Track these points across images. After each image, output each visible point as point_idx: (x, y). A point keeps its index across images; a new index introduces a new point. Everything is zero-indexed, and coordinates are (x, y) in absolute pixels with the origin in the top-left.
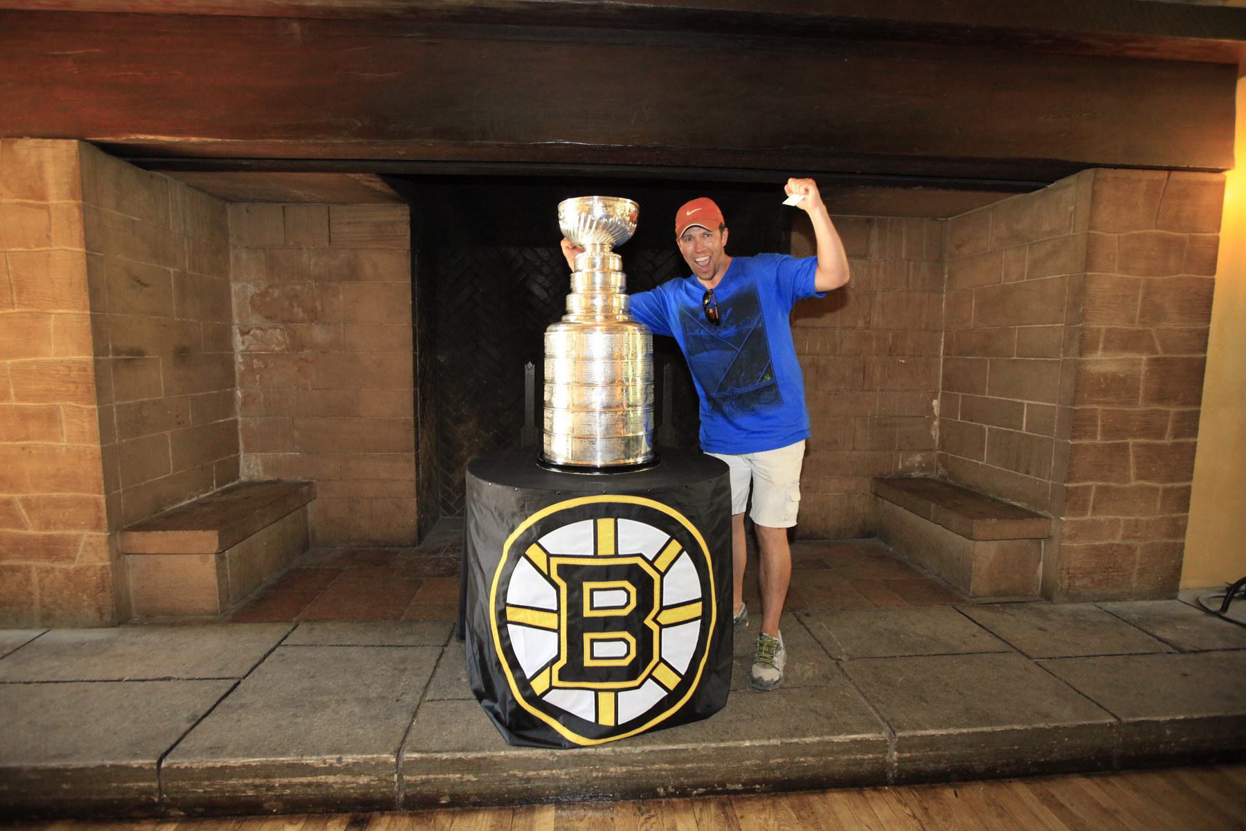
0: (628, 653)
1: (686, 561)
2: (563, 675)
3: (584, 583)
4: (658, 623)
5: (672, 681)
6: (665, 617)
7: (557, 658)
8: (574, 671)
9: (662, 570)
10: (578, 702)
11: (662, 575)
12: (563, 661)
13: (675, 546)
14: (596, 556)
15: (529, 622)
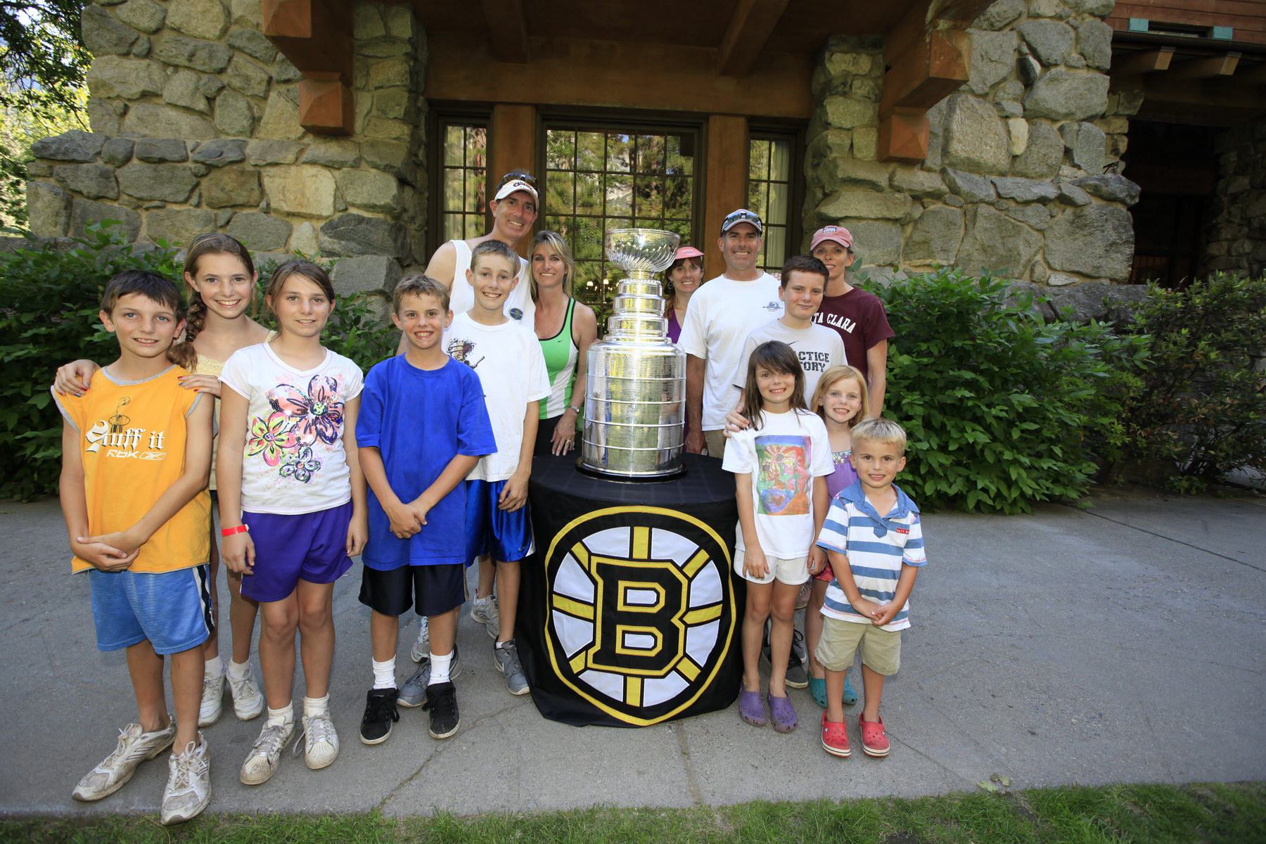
0: (655, 646)
1: (712, 569)
2: (598, 658)
3: (620, 582)
4: (684, 623)
5: (693, 673)
6: (690, 618)
7: (592, 644)
8: (607, 656)
9: (690, 575)
10: (608, 682)
11: (690, 580)
12: (597, 647)
13: (704, 555)
14: (631, 559)
15: (569, 611)
